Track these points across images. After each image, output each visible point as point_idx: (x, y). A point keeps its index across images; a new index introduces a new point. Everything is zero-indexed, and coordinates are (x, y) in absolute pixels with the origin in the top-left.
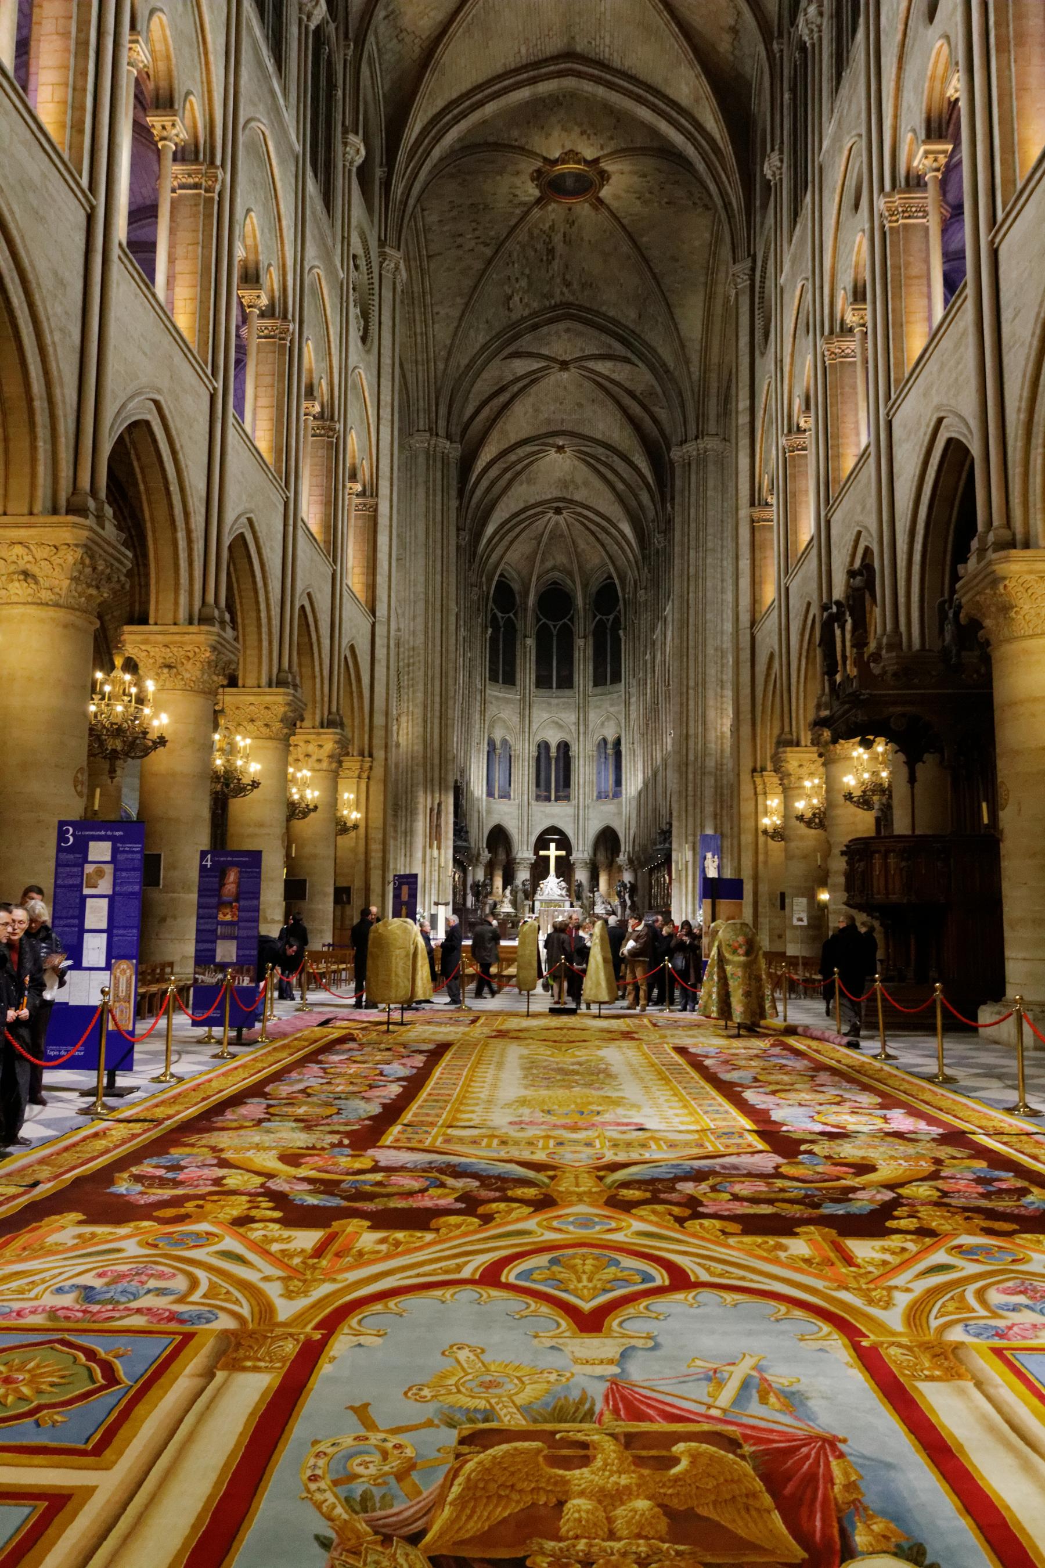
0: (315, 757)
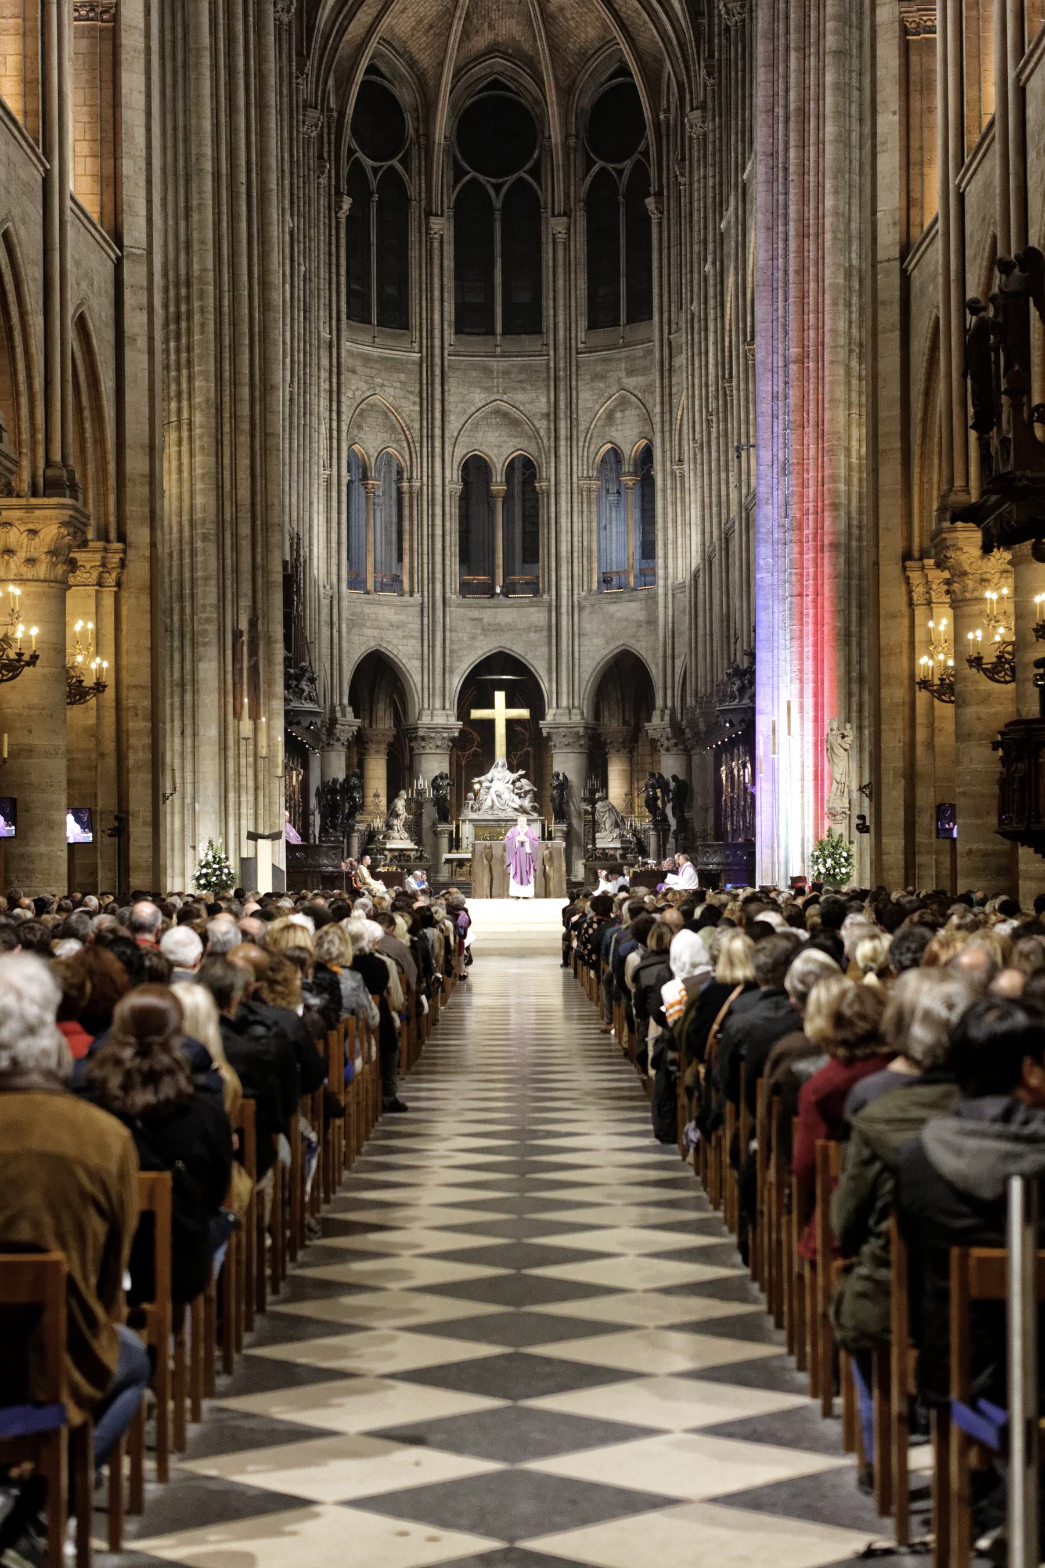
0: (22, 555)
